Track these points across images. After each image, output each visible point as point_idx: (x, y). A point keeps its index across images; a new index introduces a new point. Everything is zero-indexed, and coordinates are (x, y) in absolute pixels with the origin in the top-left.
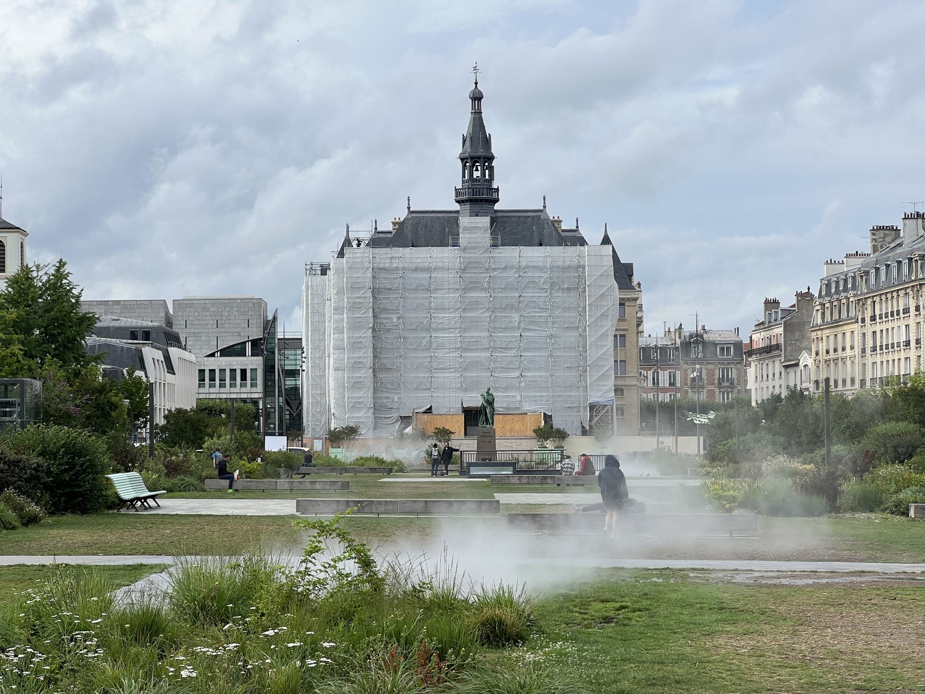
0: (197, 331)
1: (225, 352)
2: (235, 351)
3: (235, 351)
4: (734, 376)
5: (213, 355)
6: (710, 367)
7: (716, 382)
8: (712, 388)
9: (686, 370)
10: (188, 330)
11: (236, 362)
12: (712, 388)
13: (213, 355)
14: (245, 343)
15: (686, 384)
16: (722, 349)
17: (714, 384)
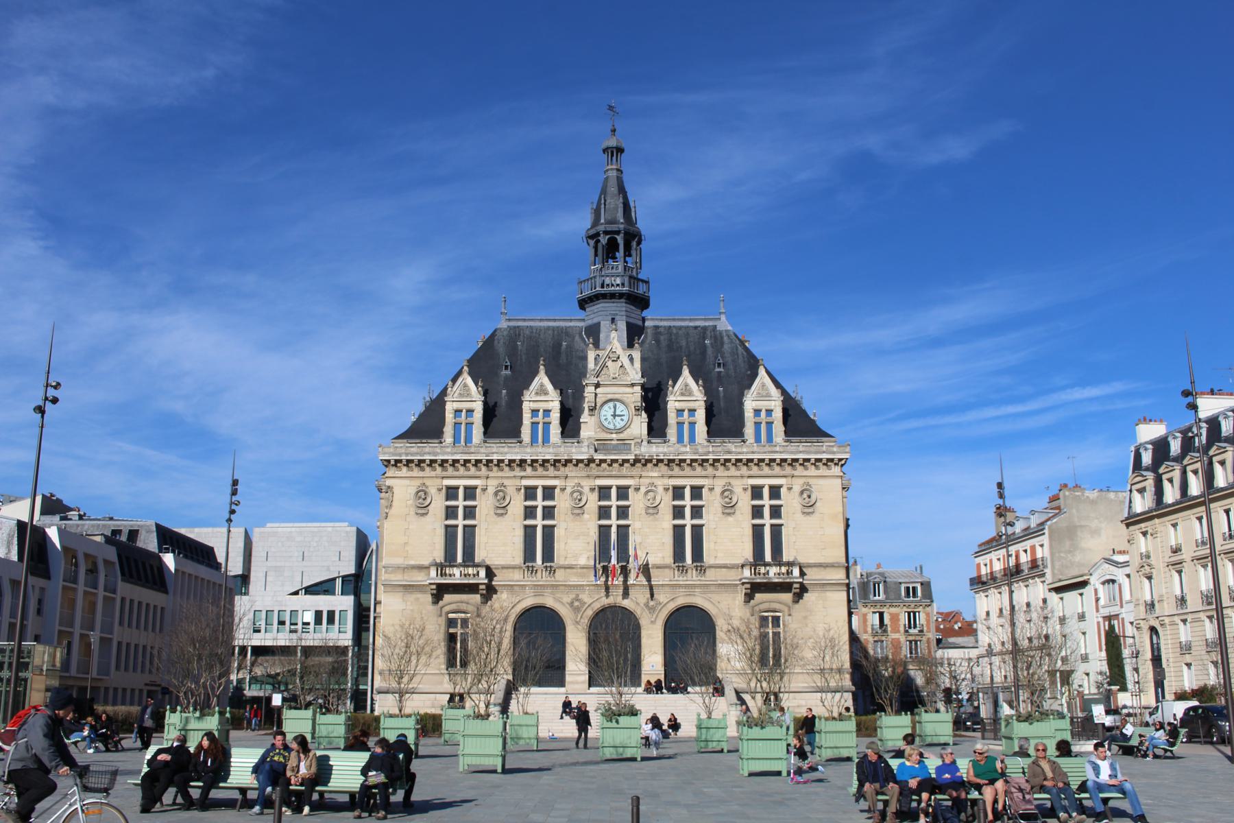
0: (279, 564)
1: (311, 590)
2: (322, 588)
3: (322, 588)
4: (923, 621)
5: (296, 593)
6: (893, 610)
7: (902, 629)
8: (896, 636)
9: (865, 615)
10: (269, 564)
11: (323, 602)
12: (896, 636)
13: (296, 593)
14: (334, 579)
15: (866, 632)
16: (908, 588)
17: (898, 631)
